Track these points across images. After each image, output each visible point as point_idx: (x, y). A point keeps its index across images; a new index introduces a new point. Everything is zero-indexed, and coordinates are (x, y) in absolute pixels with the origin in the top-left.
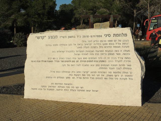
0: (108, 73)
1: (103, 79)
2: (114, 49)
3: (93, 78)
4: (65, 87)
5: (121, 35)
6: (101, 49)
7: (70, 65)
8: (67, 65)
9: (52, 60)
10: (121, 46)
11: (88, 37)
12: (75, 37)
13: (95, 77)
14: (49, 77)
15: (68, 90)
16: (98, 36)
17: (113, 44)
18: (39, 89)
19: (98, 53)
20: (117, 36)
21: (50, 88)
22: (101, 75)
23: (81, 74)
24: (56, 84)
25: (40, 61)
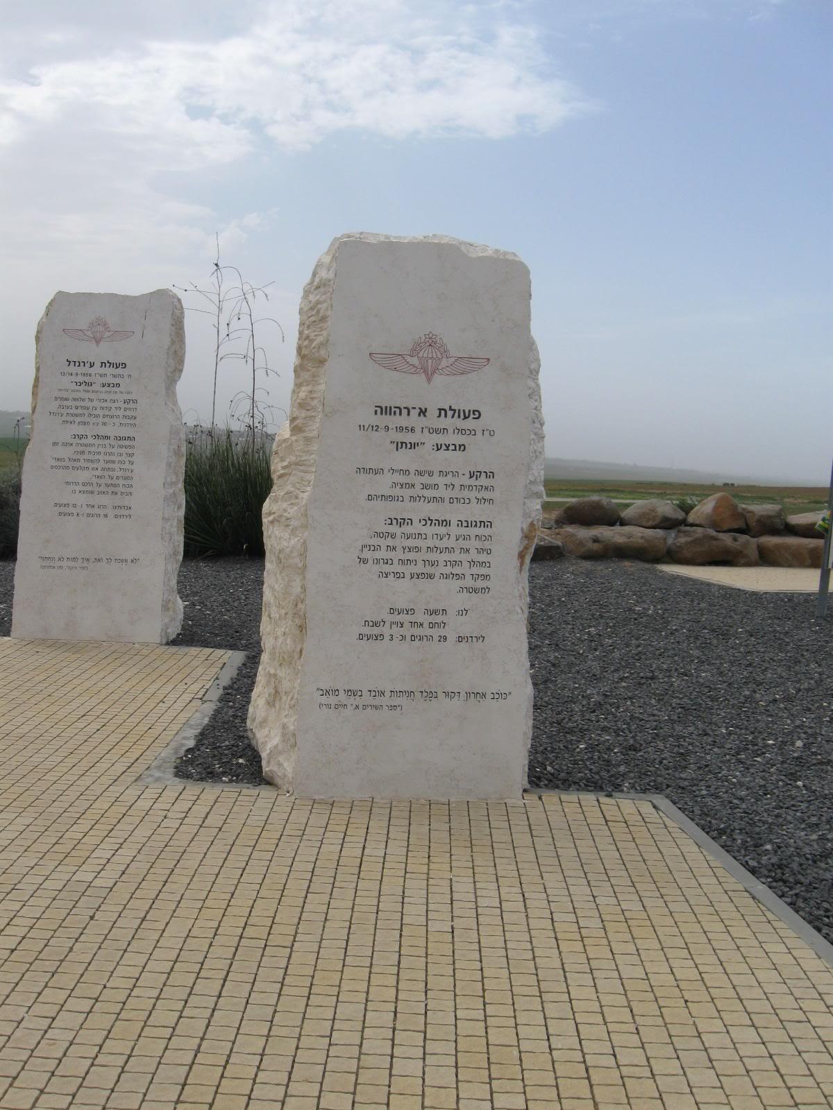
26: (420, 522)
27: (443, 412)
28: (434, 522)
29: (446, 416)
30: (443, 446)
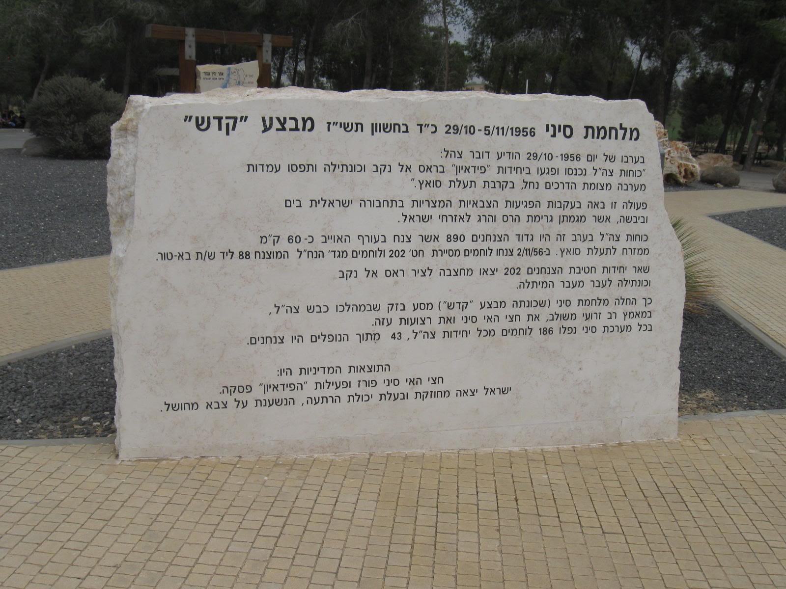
0: (555, 308)
1: (536, 332)
2: (585, 196)
3: (490, 333)
4: (354, 384)
5: (616, 130)
6: (530, 195)
7: (381, 273)
8: (362, 274)
9: (283, 246)
10: (615, 180)
11: (470, 130)
12: (407, 131)
13: (497, 327)
14: (265, 340)
15: (369, 397)
16: (518, 131)
17: (584, 173)
18: (209, 405)
19: (514, 212)
20: (598, 137)
21: (271, 395)
22: (524, 318)
23: (435, 314)
24: (307, 371)
25: (211, 256)
30: (275, 121)
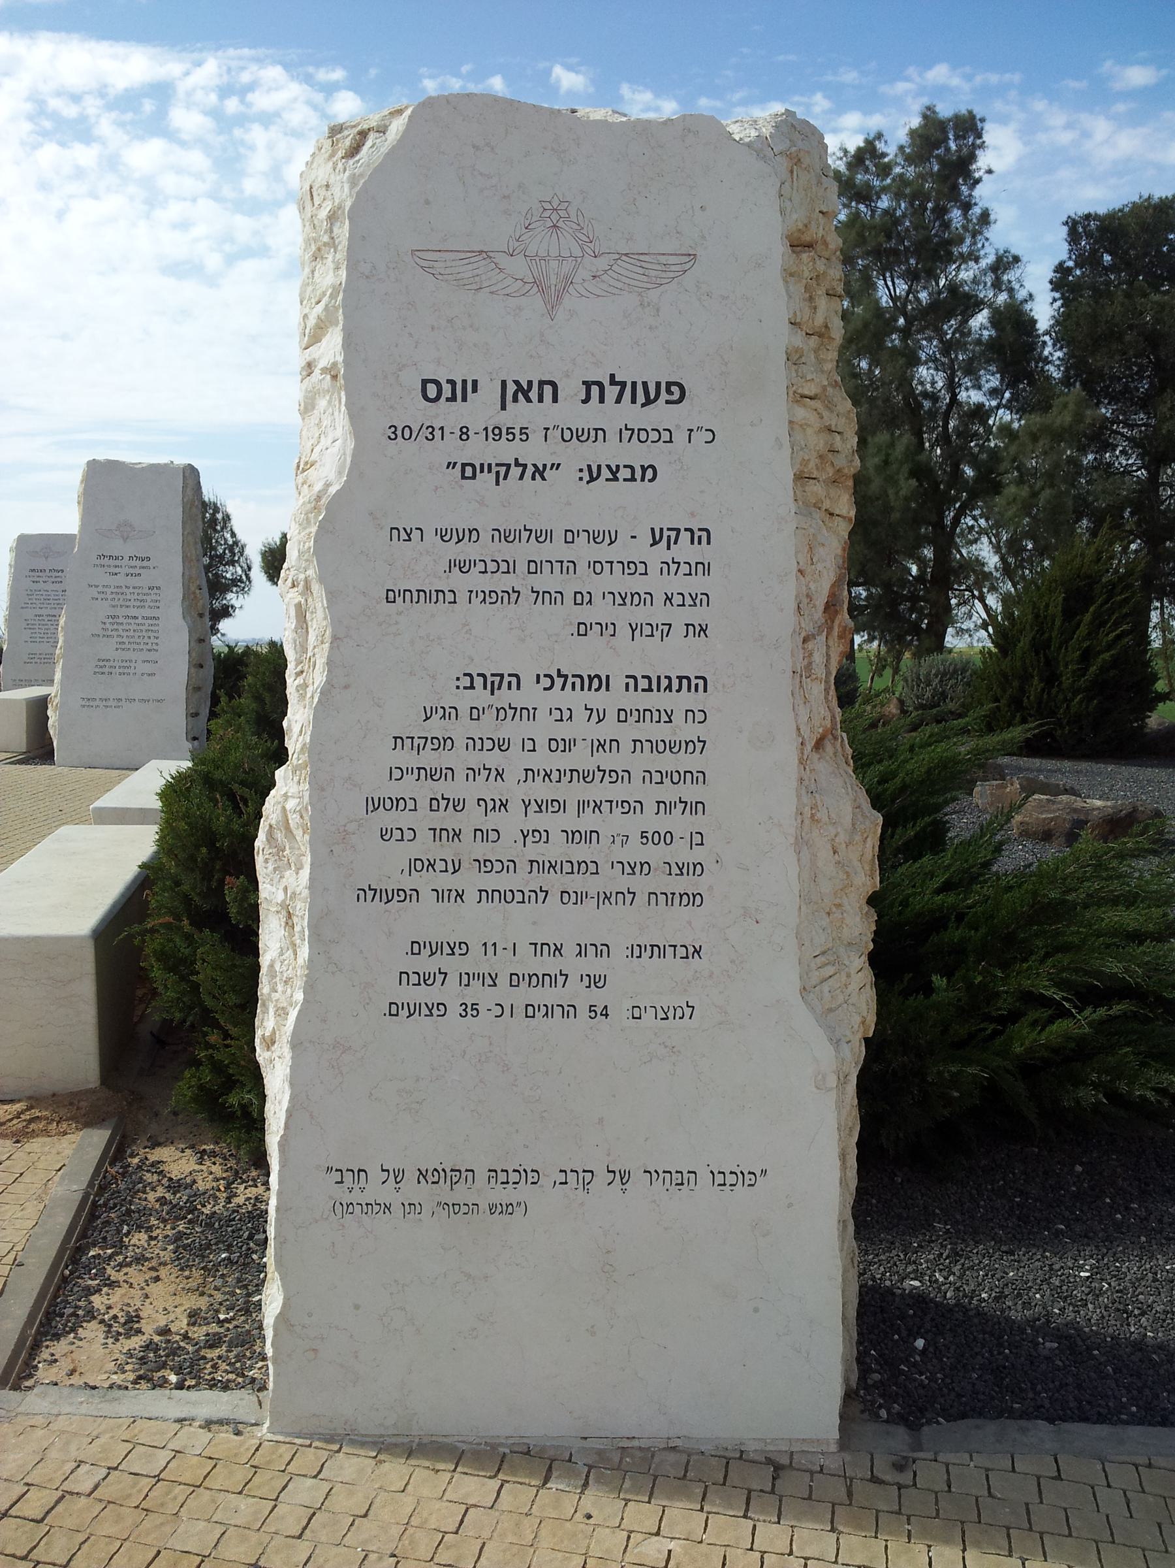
26: (538, 682)
27: (595, 390)
28: (570, 680)
29: (602, 400)
